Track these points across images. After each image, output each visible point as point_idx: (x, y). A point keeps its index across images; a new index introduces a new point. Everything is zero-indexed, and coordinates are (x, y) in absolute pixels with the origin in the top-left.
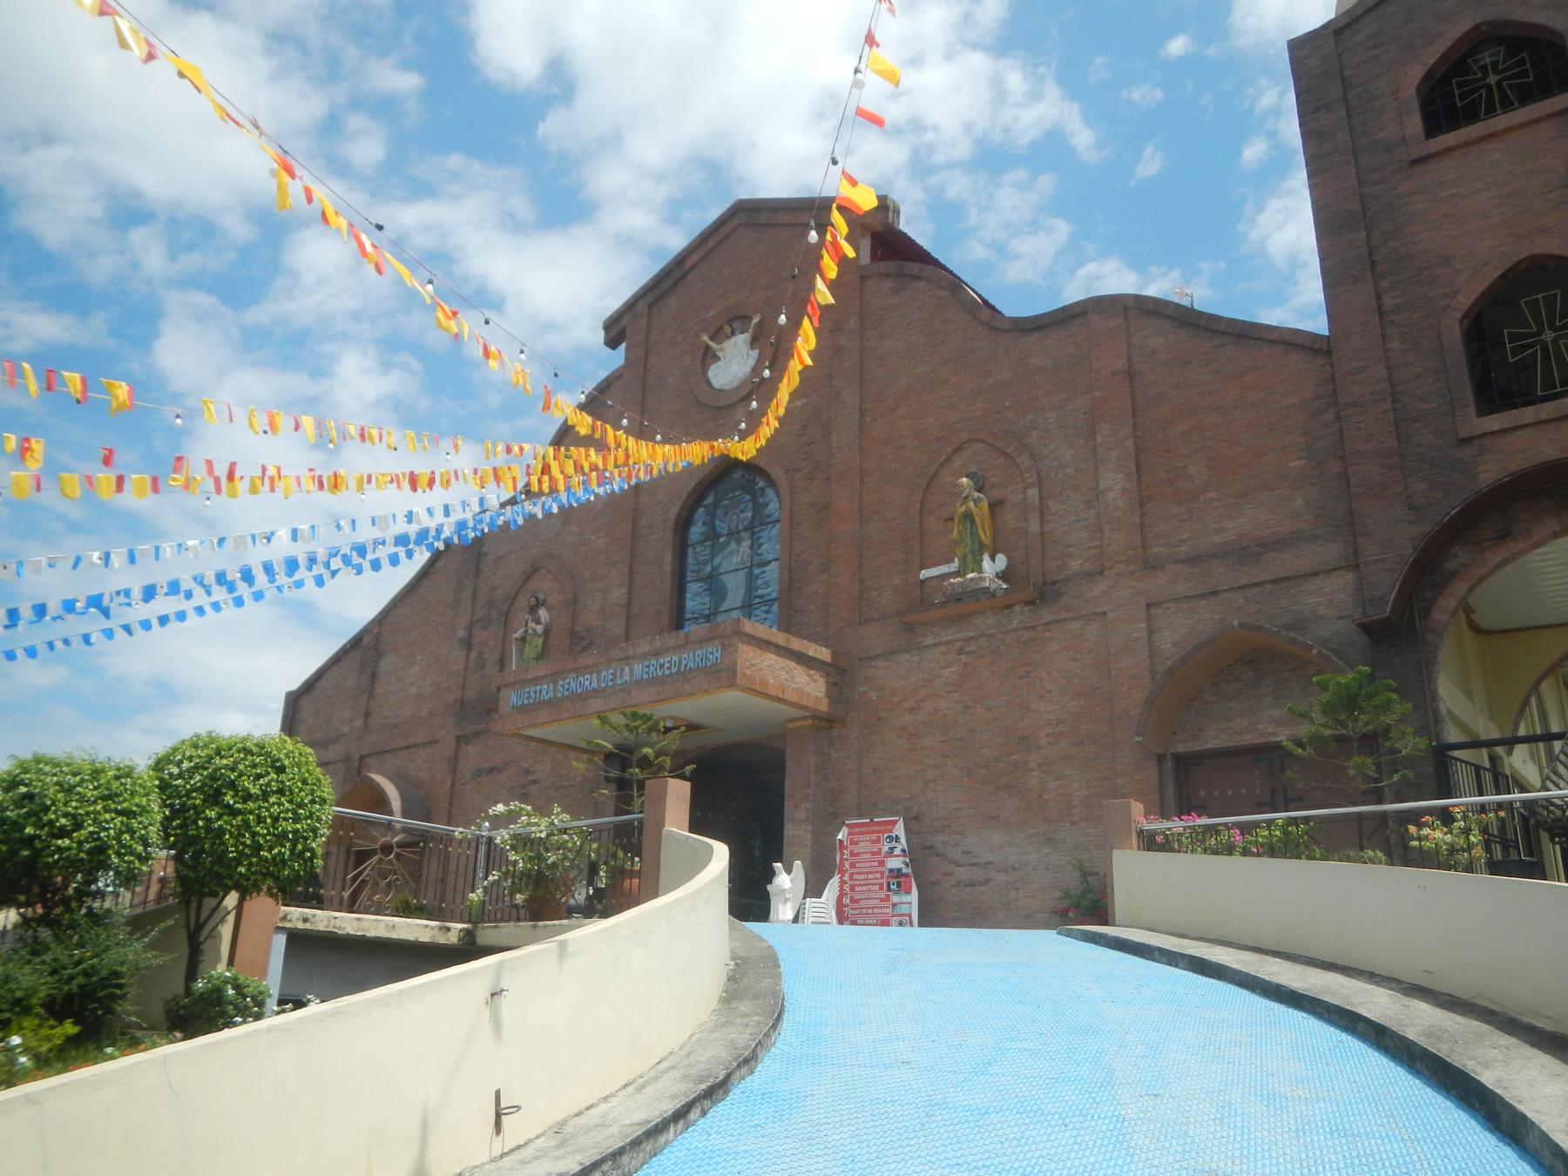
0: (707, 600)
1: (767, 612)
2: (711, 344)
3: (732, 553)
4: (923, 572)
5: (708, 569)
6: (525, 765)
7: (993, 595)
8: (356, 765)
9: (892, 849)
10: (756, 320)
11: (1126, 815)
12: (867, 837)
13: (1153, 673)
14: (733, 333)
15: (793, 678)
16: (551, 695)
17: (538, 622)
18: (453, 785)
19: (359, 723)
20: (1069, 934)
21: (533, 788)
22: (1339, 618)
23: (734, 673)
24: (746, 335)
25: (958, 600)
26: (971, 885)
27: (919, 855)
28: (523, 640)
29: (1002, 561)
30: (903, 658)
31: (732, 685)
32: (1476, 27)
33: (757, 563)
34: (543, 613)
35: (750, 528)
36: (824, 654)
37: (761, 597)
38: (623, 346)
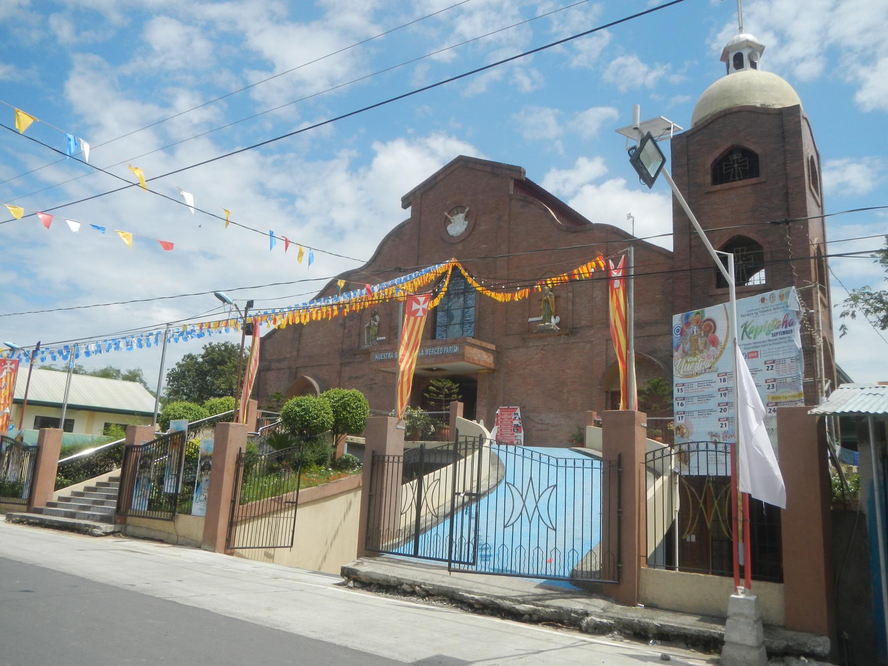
0: (446, 319)
1: (470, 327)
2: (449, 216)
3: (456, 302)
5: (446, 307)
6: (371, 377)
7: (555, 332)
8: (294, 371)
10: (467, 209)
11: (591, 415)
12: (506, 413)
13: (606, 363)
14: (458, 213)
16: (392, 357)
17: (376, 321)
18: (339, 382)
19: (295, 354)
20: (572, 450)
21: (374, 386)
22: (667, 351)
23: (464, 356)
24: (463, 214)
25: (542, 332)
26: (542, 430)
27: (524, 419)
28: (369, 327)
29: (558, 319)
30: (521, 350)
31: (463, 360)
32: (733, 146)
33: (465, 307)
34: (377, 317)
35: (464, 293)
36: (493, 347)
38: (410, 207)
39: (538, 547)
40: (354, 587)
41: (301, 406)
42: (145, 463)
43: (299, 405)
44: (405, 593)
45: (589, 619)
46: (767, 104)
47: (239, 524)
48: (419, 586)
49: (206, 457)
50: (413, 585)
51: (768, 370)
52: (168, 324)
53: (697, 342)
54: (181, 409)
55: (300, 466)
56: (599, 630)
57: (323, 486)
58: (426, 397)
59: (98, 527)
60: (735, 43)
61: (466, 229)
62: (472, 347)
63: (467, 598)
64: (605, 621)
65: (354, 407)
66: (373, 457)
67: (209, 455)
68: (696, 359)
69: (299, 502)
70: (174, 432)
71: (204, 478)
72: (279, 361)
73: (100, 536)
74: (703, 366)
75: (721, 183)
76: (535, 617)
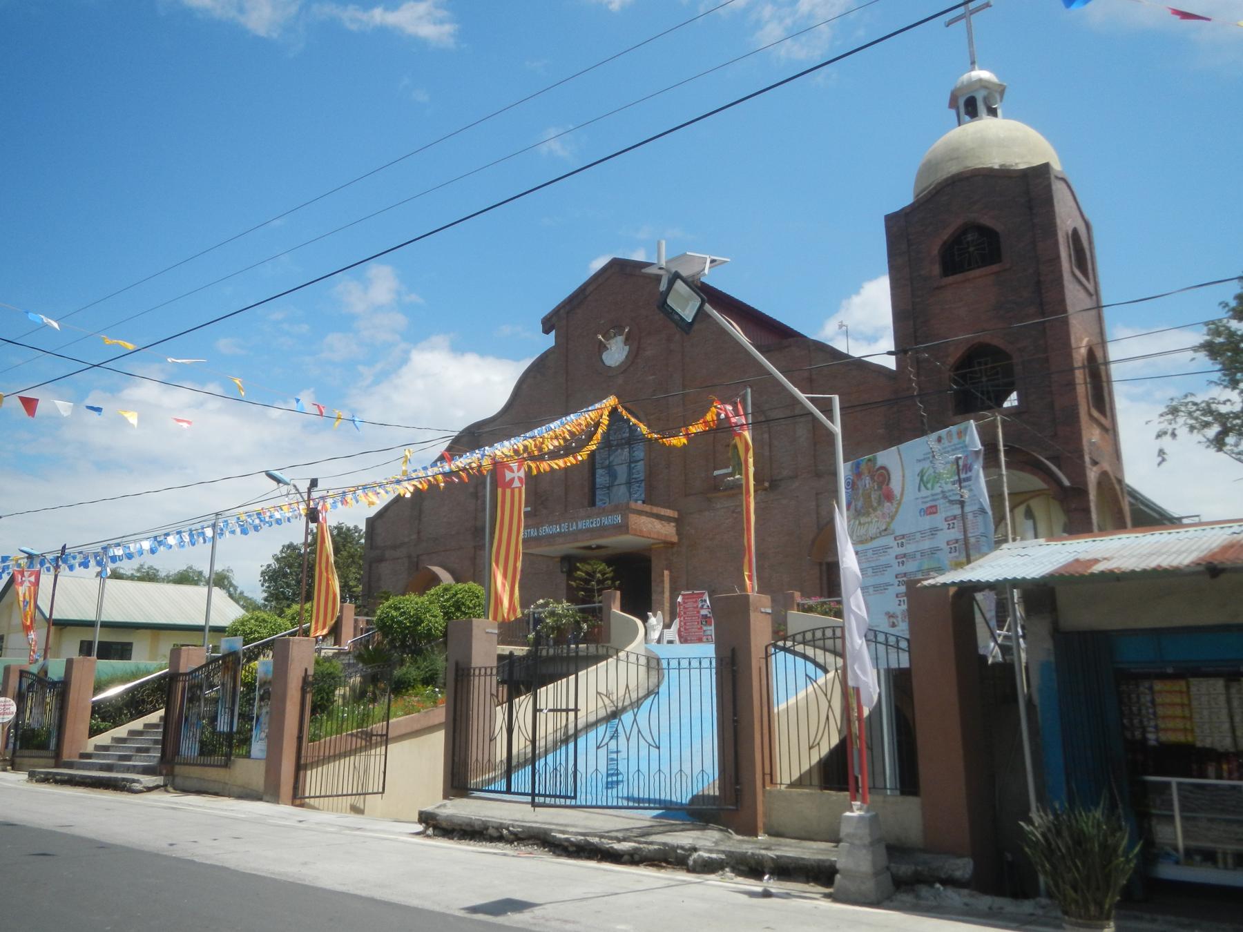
0: (608, 478)
1: (639, 487)
4: (715, 472)
5: (607, 462)
9: (703, 606)
11: (792, 596)
12: (691, 600)
14: (615, 336)
15: (654, 526)
19: (414, 537)
23: (628, 528)
24: (621, 337)
25: (732, 488)
33: (632, 461)
37: (635, 479)
38: (554, 332)
39: (638, 770)
40: (435, 835)
41: (400, 609)
42: (193, 694)
43: (397, 609)
44: (492, 839)
45: (695, 855)
46: (1008, 164)
47: (309, 767)
48: (507, 829)
49: (265, 682)
50: (499, 827)
51: (949, 529)
52: (217, 514)
53: (870, 497)
54: (253, 621)
55: (400, 687)
56: (708, 867)
57: (426, 712)
58: (572, 585)
59: (138, 781)
60: (965, 83)
61: (626, 357)
62: (639, 515)
63: (560, 839)
64: (714, 856)
65: (471, 605)
66: (457, 670)
67: (268, 680)
68: (869, 519)
69: (390, 736)
70: (226, 652)
71: (264, 710)
72: (394, 547)
73: (140, 792)
74: (878, 528)
75: (953, 274)
76: (637, 857)
